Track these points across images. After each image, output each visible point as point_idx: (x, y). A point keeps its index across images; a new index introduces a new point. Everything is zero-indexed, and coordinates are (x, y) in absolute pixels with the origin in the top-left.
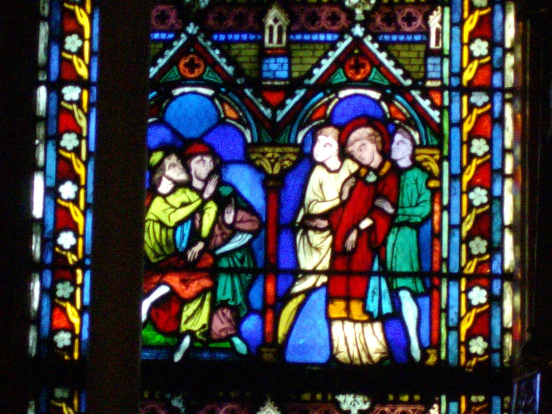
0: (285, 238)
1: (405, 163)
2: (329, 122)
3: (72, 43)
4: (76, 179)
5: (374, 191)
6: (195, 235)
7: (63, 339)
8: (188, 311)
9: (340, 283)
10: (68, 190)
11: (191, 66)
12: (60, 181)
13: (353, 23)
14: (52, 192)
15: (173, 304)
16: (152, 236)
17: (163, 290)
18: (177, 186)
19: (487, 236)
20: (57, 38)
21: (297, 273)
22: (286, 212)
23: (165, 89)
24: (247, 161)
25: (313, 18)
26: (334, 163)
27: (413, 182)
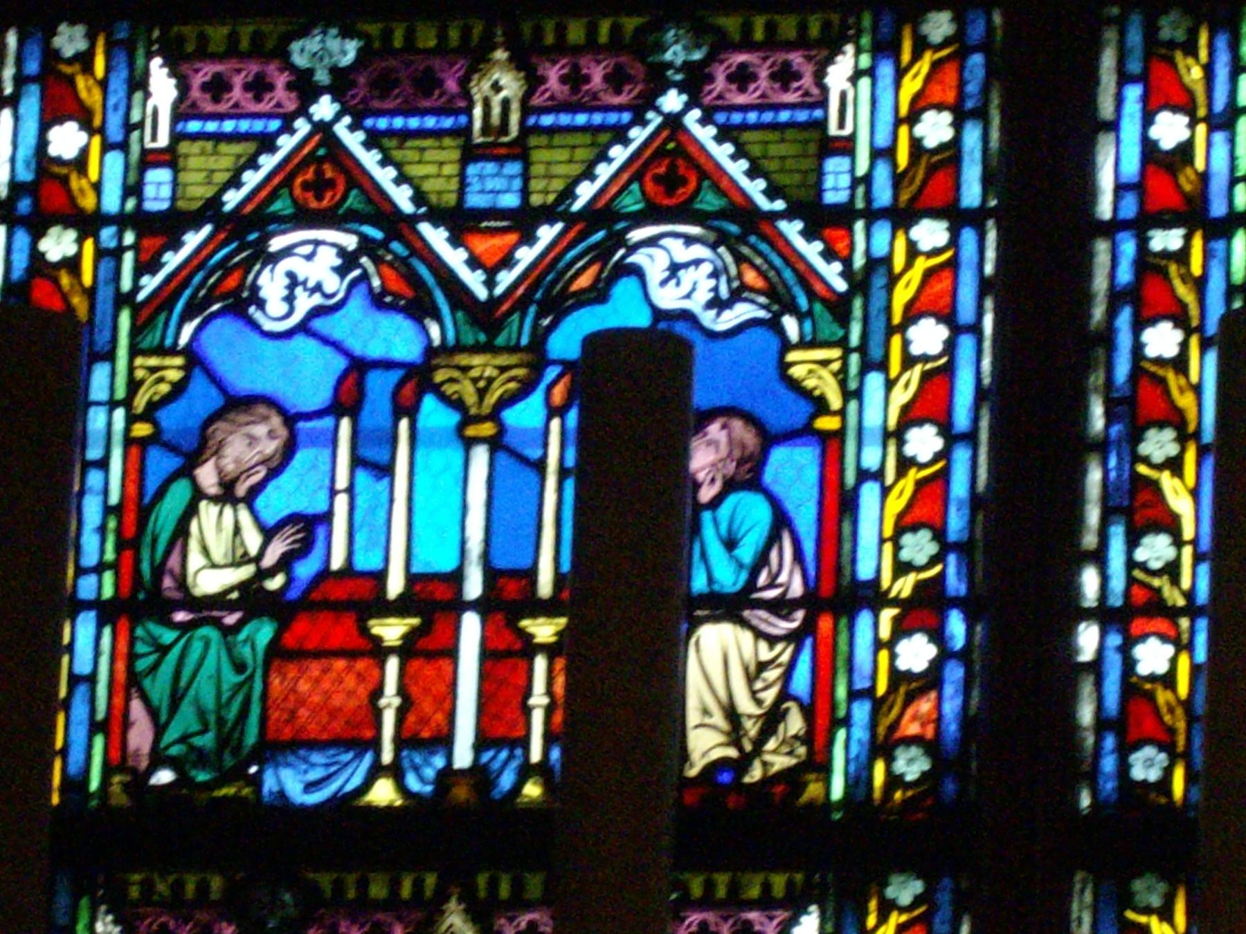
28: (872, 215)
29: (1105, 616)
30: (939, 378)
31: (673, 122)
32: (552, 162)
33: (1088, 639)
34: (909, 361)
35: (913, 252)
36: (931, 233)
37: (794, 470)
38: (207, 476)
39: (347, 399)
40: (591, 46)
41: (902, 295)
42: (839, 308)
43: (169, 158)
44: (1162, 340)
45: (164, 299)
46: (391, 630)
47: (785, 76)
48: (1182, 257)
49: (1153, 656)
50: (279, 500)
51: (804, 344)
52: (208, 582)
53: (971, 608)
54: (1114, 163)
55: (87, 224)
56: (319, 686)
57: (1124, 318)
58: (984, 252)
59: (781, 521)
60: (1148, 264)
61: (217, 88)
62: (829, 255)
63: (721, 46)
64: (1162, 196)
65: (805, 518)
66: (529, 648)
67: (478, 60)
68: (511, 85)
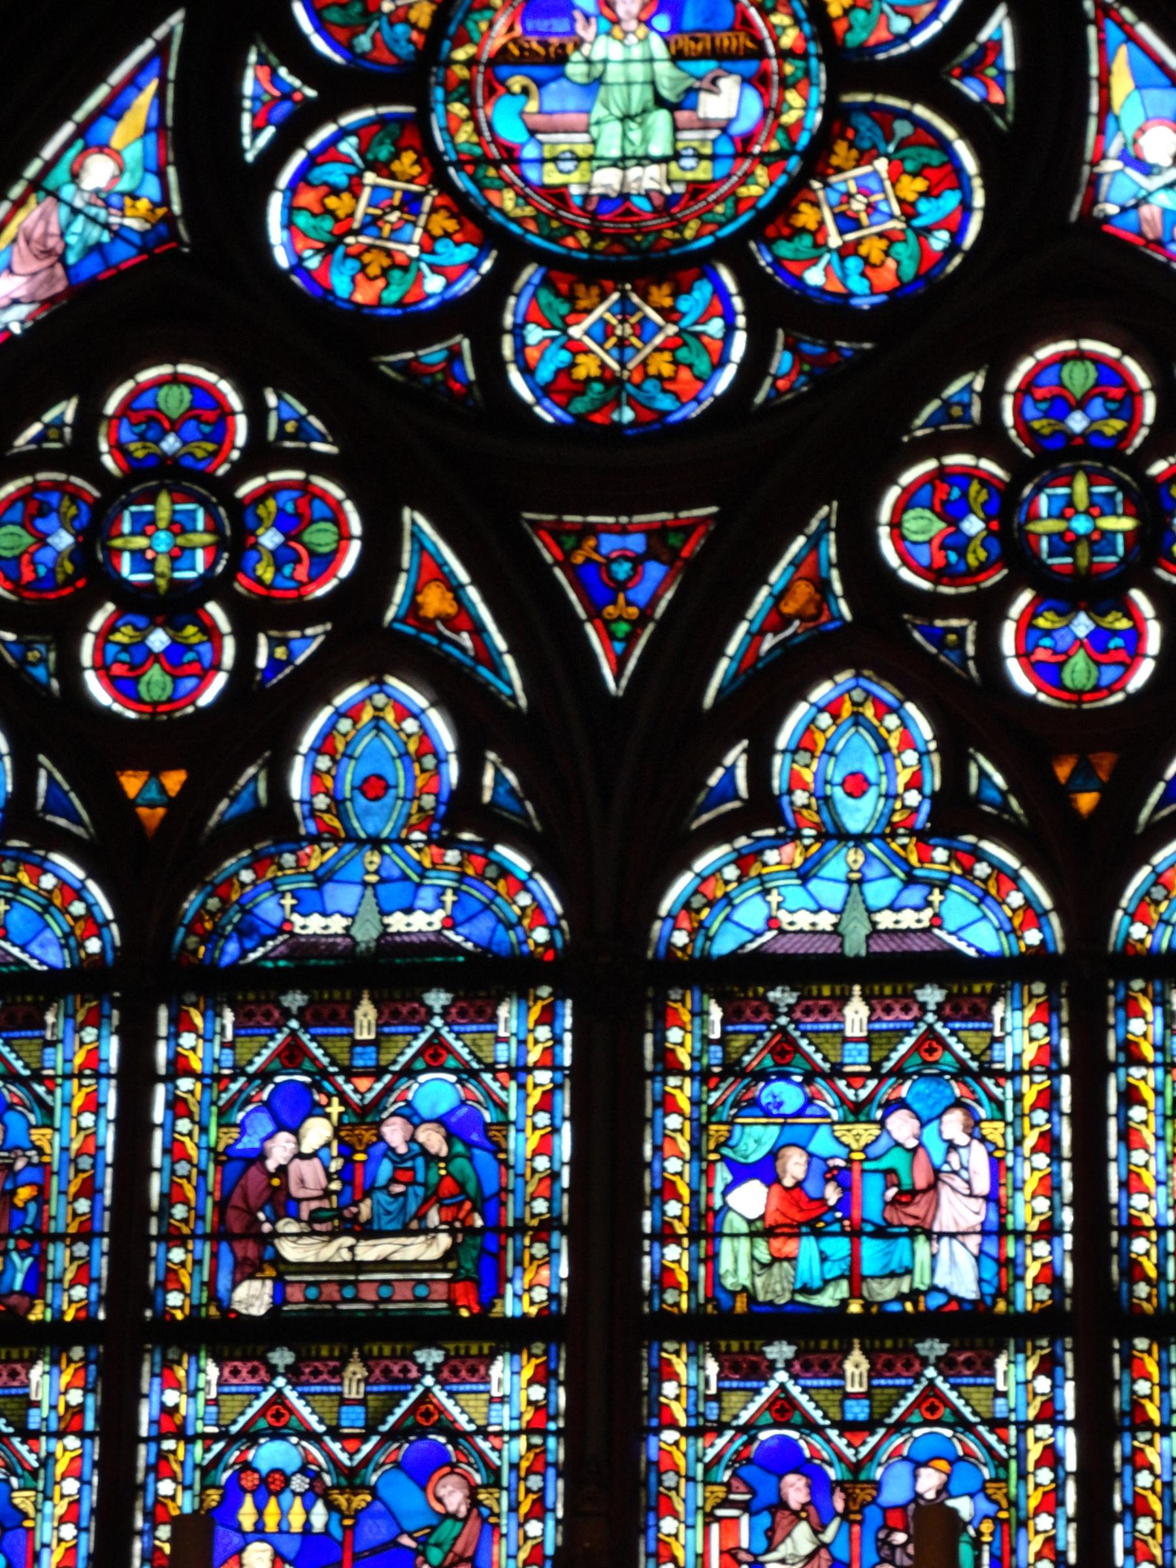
28: (50, 1435)
30: (75, 1504)
34: (62, 1496)
35: (65, 1450)
36: (72, 1442)
41: (60, 1468)
42: (34, 1473)
44: (166, 1487)
48: (174, 1452)
51: (20, 1489)
54: (146, 1413)
57: (152, 1477)
58: (94, 1450)
60: (162, 1456)
62: (31, 1451)
64: (167, 1427)
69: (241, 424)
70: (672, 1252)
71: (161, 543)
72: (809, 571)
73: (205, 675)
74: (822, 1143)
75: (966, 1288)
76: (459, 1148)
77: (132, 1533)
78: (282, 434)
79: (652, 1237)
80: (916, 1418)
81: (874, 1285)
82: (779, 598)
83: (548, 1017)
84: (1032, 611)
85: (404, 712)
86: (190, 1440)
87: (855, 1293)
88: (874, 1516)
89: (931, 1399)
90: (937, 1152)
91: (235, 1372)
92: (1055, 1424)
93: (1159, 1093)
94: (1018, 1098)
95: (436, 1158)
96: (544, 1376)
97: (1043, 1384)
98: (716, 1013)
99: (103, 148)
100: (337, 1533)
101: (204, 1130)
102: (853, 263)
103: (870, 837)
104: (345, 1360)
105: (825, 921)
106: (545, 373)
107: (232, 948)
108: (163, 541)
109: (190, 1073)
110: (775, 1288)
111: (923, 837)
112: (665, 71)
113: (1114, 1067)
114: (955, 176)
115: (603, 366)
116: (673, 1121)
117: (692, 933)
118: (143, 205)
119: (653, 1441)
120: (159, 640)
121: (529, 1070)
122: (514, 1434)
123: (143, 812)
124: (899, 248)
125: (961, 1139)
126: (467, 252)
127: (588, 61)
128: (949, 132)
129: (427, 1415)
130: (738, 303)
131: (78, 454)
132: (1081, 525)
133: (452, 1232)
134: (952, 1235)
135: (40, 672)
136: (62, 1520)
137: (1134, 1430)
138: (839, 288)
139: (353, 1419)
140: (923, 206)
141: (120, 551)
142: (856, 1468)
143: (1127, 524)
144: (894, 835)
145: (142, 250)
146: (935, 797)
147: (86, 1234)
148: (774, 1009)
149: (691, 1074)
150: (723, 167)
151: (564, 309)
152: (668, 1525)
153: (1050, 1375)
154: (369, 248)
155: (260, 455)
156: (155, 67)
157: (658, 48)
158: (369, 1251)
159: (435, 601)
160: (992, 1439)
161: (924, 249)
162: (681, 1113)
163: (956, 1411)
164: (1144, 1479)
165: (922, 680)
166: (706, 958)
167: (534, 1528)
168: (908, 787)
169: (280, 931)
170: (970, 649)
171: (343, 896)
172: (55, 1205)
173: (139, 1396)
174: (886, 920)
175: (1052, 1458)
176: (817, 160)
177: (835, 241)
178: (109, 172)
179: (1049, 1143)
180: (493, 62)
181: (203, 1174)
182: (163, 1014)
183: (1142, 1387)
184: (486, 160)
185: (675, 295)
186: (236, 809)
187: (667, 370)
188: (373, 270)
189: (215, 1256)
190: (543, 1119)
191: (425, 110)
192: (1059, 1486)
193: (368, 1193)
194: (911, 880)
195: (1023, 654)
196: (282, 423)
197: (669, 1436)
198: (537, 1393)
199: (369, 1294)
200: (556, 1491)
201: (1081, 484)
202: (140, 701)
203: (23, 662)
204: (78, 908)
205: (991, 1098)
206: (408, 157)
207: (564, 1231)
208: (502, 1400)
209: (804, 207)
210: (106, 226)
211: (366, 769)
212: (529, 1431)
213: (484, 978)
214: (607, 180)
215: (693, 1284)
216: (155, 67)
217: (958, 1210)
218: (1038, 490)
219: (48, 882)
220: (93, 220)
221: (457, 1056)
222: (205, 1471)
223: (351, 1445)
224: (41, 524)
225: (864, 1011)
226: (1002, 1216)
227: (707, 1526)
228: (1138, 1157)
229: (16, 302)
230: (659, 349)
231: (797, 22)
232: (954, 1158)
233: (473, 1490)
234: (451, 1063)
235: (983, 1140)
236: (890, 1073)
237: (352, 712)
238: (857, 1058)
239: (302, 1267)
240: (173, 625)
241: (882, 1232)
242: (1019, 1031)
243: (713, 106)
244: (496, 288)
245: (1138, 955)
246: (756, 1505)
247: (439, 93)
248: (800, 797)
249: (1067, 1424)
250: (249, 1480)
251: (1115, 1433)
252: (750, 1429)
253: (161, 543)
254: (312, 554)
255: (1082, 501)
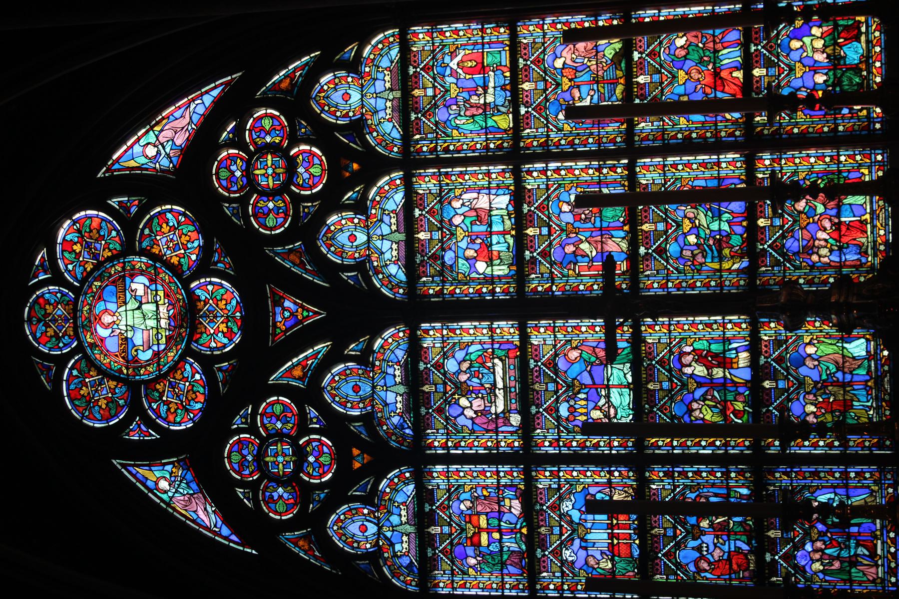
0: (714, 381)
1: (691, 348)
2: (680, 370)
3: (660, 443)
4: (700, 441)
5: (701, 357)
6: (715, 407)
7: (747, 443)
8: (737, 408)
9: (728, 365)
10: (703, 443)
11: (666, 409)
12: (701, 445)
13: (651, 364)
14: (704, 448)
15: (737, 413)
16: (717, 419)
17: (731, 415)
18: (701, 412)
19: (712, 324)
20: (659, 448)
21: (725, 377)
22: (708, 381)
23: (673, 417)
24: (693, 392)
25: (651, 375)
26: (693, 368)
27: (697, 345)
29: (611, 450)
31: (547, 507)
32: (553, 523)
33: (614, 452)
36: (561, 474)
37: (592, 490)
38: (596, 566)
39: (585, 548)
40: (538, 518)
43: (554, 573)
44: (574, 444)
45: (572, 573)
46: (615, 541)
47: (541, 493)
49: (616, 444)
50: (599, 557)
52: (610, 566)
53: (610, 467)
54: (551, 451)
55: (563, 583)
56: (623, 550)
58: (564, 467)
59: (599, 492)
61: (544, 567)
63: (537, 502)
64: (556, 444)
65: (600, 488)
66: (617, 524)
67: (540, 533)
68: (543, 529)
69: (242, 436)
70: (498, 290)
71: (280, 459)
72: (286, 256)
73: (323, 444)
74: (463, 245)
75: (507, 198)
76: (467, 357)
77: (589, 453)
78: (246, 423)
79: (493, 296)
80: (547, 213)
81: (506, 227)
82: (294, 264)
83: (426, 332)
84: (297, 185)
85: (333, 380)
86: (560, 436)
87: (509, 233)
88: (577, 224)
89: (541, 208)
90: (465, 209)
91: (538, 424)
92: (547, 170)
93: (445, 142)
94: (447, 184)
95: (471, 364)
96: (537, 328)
97: (535, 174)
98: (424, 279)
99: (156, 483)
100: (586, 390)
101: (464, 437)
102: (189, 246)
103: (368, 233)
104: (534, 390)
105: (395, 246)
106: (225, 341)
107: (407, 431)
108: (280, 459)
109: (446, 443)
110: (507, 256)
111: (368, 218)
112: (129, 307)
113: (437, 155)
114: (161, 214)
115: (222, 322)
116: (458, 291)
117: (400, 287)
118: (174, 470)
119: (556, 293)
120: (311, 459)
121: (443, 336)
122: (555, 336)
123: (365, 461)
124: (184, 231)
125: (461, 202)
126: (188, 367)
127: (126, 331)
128: (148, 216)
129: (550, 364)
130: (203, 280)
131: (253, 486)
132: (270, 171)
133: (493, 358)
134: (490, 203)
135: (322, 496)
136: (585, 476)
137: (549, 146)
138: (197, 251)
139: (551, 387)
140: (171, 224)
141: (284, 472)
142: (562, 230)
143: (269, 157)
144: (368, 226)
145: (188, 470)
146: (355, 214)
147: (498, 472)
148: (422, 261)
149: (443, 286)
150: (160, 287)
151: (205, 335)
152: (581, 287)
153: (532, 172)
154: (187, 398)
155: (252, 429)
156: (131, 469)
157: (123, 308)
158: (500, 384)
159: (298, 372)
160: (552, 189)
161: (184, 223)
162: (455, 289)
163: (544, 200)
164: (563, 142)
165: (319, 219)
166: (407, 283)
167: (583, 329)
168: (353, 222)
169: (402, 416)
170: (310, 204)
171: (390, 397)
172: (489, 482)
173: (547, 454)
174: (394, 227)
175: (557, 171)
176: (157, 258)
177: (182, 251)
178: (164, 482)
179: (461, 175)
180: (128, 361)
181: (477, 437)
182: (428, 452)
183: (535, 143)
184: (158, 363)
185: (200, 301)
186: (364, 432)
187: (224, 302)
188: (194, 396)
189: (503, 432)
190: (458, 332)
191: (143, 381)
192: (566, 169)
193: (482, 385)
194: (381, 220)
195: (311, 188)
196: (242, 423)
197: (554, 288)
198: (542, 330)
199: (513, 384)
200: (572, 322)
201: (257, 172)
202: (330, 464)
203: (319, 501)
204: (396, 480)
205: (448, 193)
206: (158, 386)
207: (492, 324)
208: (545, 341)
209: (172, 261)
210: (181, 481)
211: (351, 392)
212: (554, 332)
213: (415, 350)
214: (163, 323)
215: (508, 283)
216: (131, 469)
217: (483, 202)
218: (259, 185)
219: (388, 490)
220: (179, 485)
221: (439, 359)
222: (569, 432)
223: (560, 387)
224: (276, 498)
225: (422, 233)
226: (484, 188)
227: (582, 276)
228: (465, 147)
229: (205, 509)
230: (217, 305)
231: (114, 266)
232: (467, 204)
233: (573, 348)
234: (441, 361)
235: (461, 195)
236: (441, 224)
237: (333, 396)
238: (437, 235)
239: (505, 405)
240: (307, 454)
241: (490, 226)
242: (426, 184)
243: (140, 292)
244: (199, 357)
245: (403, 149)
246: (574, 261)
247: (137, 377)
248: (357, 255)
249: (547, 167)
250: (571, 418)
251: (549, 151)
252: (552, 263)
253: (280, 459)
254: (283, 412)
255: (263, 171)
